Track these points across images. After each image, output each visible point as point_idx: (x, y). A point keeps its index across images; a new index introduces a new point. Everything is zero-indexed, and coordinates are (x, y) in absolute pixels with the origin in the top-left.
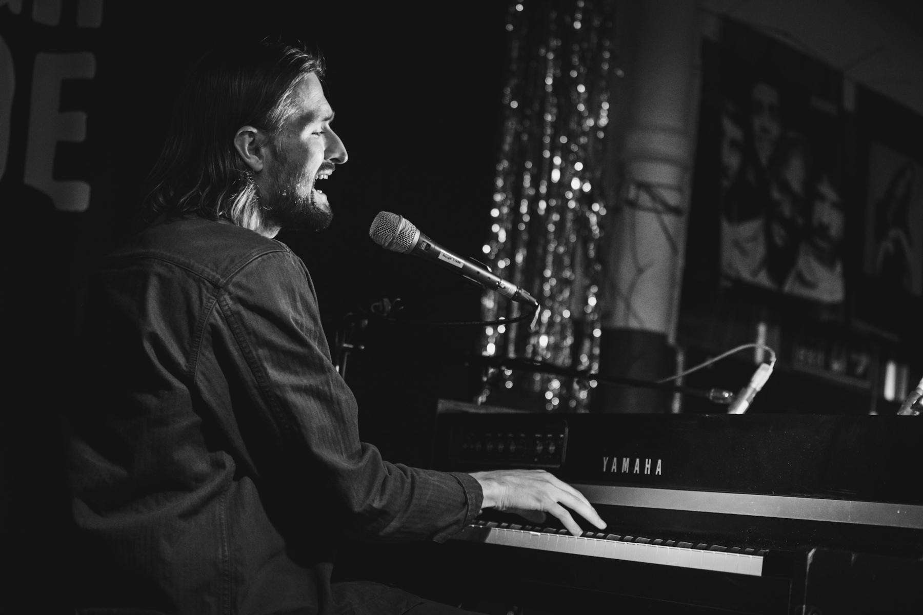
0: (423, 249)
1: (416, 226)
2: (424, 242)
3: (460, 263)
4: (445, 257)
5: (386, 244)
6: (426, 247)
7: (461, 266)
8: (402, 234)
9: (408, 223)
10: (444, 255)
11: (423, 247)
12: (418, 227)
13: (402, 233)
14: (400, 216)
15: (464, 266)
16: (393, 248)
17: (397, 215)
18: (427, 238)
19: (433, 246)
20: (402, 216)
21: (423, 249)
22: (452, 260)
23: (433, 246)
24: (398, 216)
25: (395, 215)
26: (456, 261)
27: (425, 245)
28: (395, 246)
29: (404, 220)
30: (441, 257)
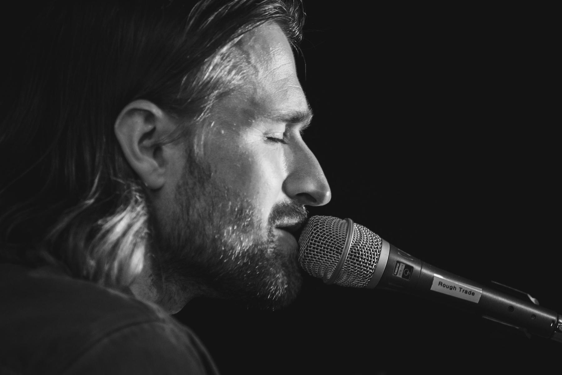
0: (400, 276)
1: (381, 237)
2: (399, 262)
3: (473, 294)
4: (444, 286)
5: (329, 276)
6: (405, 272)
7: (476, 300)
8: (355, 254)
9: (365, 231)
10: (440, 283)
11: (399, 273)
12: (385, 236)
13: (355, 254)
14: (348, 221)
15: (483, 298)
16: (344, 280)
17: (343, 218)
18: (403, 256)
19: (417, 268)
20: (351, 221)
21: (400, 276)
22: (458, 290)
23: (417, 268)
24: (344, 221)
25: (339, 219)
26: (466, 292)
27: (402, 268)
28: (345, 277)
29: (355, 226)
30: (435, 287)
